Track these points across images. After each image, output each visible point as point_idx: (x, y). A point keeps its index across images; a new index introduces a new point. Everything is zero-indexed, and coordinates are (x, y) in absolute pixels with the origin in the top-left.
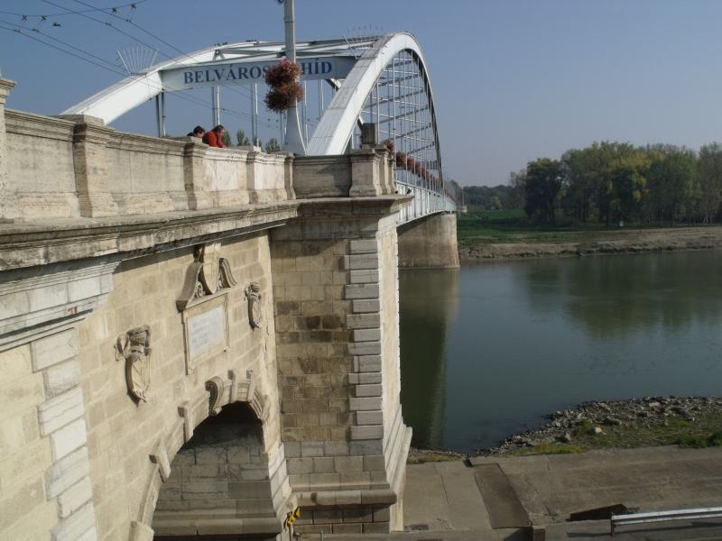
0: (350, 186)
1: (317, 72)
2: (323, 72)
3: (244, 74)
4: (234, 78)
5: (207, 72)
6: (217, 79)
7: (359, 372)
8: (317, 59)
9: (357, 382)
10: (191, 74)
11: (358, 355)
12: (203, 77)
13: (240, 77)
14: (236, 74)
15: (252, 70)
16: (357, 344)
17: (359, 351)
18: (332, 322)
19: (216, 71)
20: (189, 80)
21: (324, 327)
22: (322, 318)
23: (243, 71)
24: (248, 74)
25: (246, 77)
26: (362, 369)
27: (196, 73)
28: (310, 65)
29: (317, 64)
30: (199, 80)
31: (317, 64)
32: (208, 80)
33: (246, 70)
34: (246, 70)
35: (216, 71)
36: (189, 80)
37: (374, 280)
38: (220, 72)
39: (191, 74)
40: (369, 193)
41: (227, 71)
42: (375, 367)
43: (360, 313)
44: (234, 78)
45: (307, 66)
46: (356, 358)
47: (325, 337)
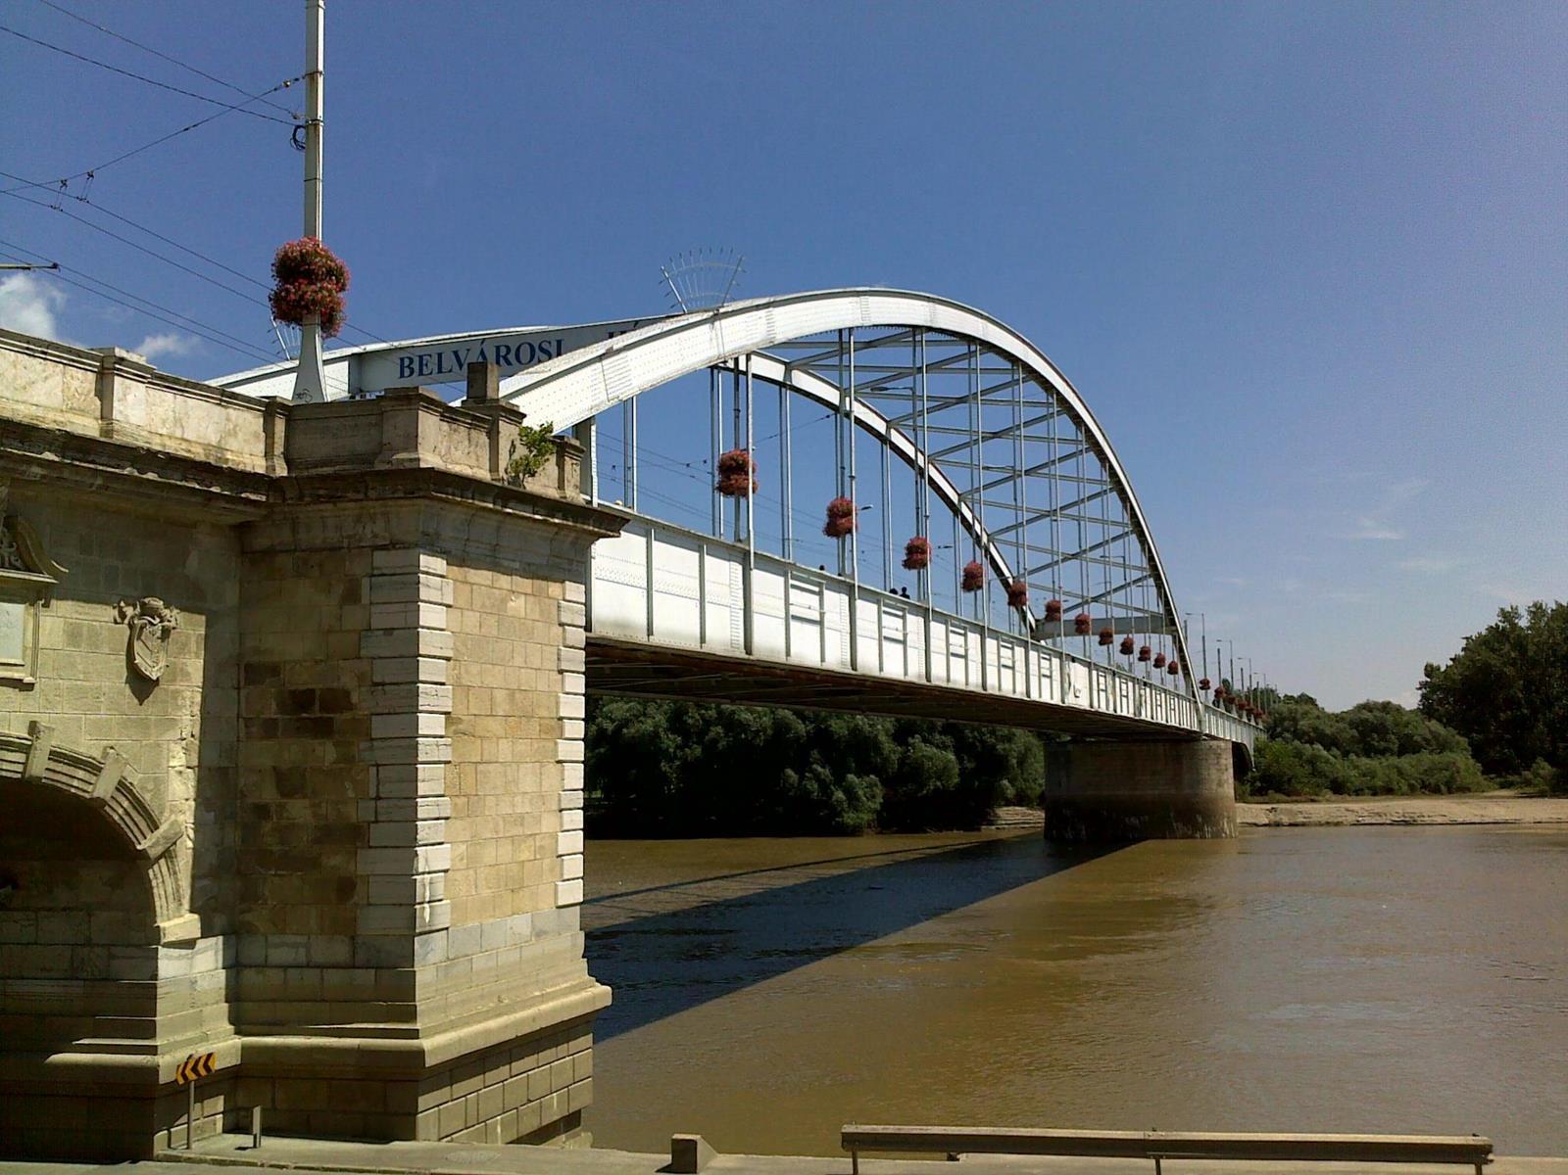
3: (505, 358)
6: (456, 368)
7: (378, 798)
9: (373, 819)
10: (411, 360)
11: (378, 765)
12: (433, 365)
15: (518, 350)
16: (375, 743)
18: (338, 700)
19: (456, 353)
20: (407, 372)
22: (318, 693)
23: (503, 351)
24: (511, 357)
25: (509, 363)
27: (421, 357)
30: (425, 371)
32: (440, 371)
35: (456, 353)
36: (407, 372)
38: (462, 356)
39: (411, 360)
43: (383, 684)
47: (323, 729)
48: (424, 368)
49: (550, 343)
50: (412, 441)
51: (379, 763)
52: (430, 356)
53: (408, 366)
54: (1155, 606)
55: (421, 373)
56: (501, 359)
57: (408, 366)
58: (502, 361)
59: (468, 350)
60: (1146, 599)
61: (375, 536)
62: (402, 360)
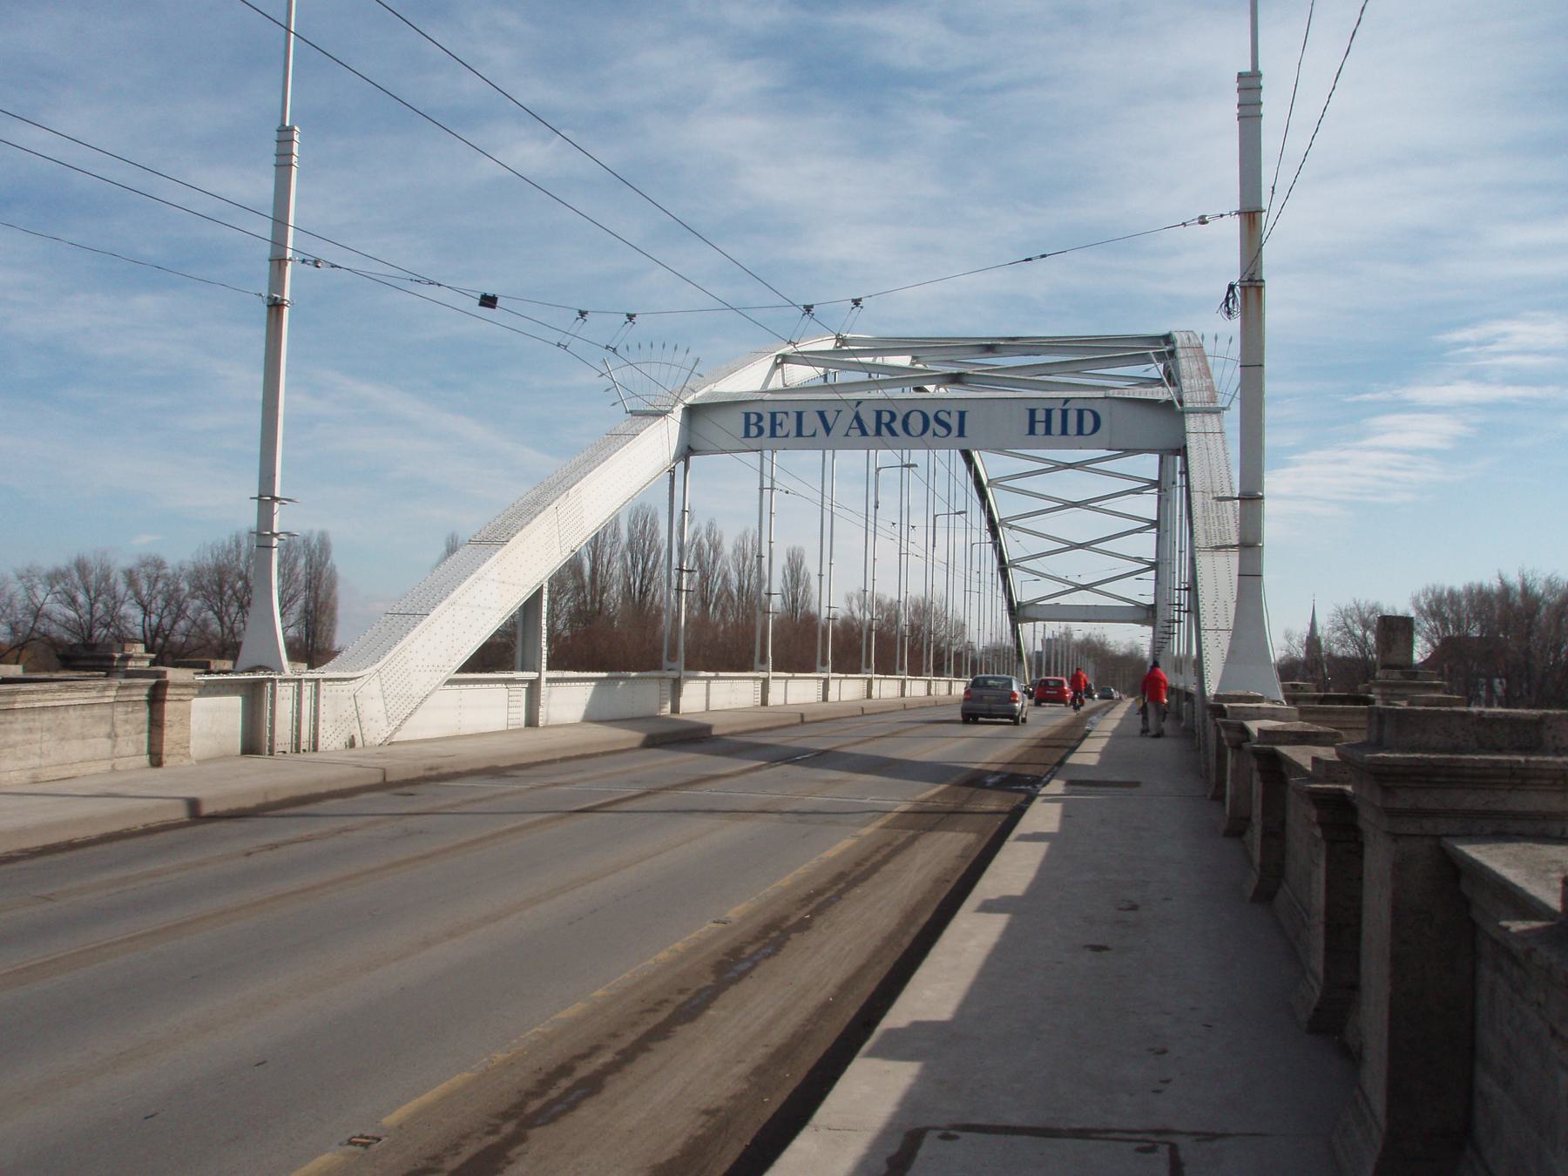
1: (1064, 432)
2: (1080, 432)
3: (888, 426)
4: (864, 433)
5: (799, 415)
6: (821, 431)
8: (1067, 400)
10: (760, 417)
12: (790, 424)
13: (878, 433)
14: (870, 424)
15: (907, 416)
19: (821, 414)
20: (754, 430)
23: (886, 418)
24: (897, 426)
25: (893, 433)
27: (773, 415)
28: (1049, 412)
29: (1065, 413)
30: (779, 431)
31: (1065, 413)
32: (799, 434)
33: (893, 417)
34: (893, 417)
35: (821, 414)
36: (754, 430)
39: (760, 417)
41: (847, 418)
44: (864, 433)
45: (1040, 416)
48: (778, 427)
49: (949, 413)
52: (786, 413)
53: (755, 424)
56: (883, 427)
57: (755, 424)
58: (884, 430)
59: (839, 412)
62: (747, 416)
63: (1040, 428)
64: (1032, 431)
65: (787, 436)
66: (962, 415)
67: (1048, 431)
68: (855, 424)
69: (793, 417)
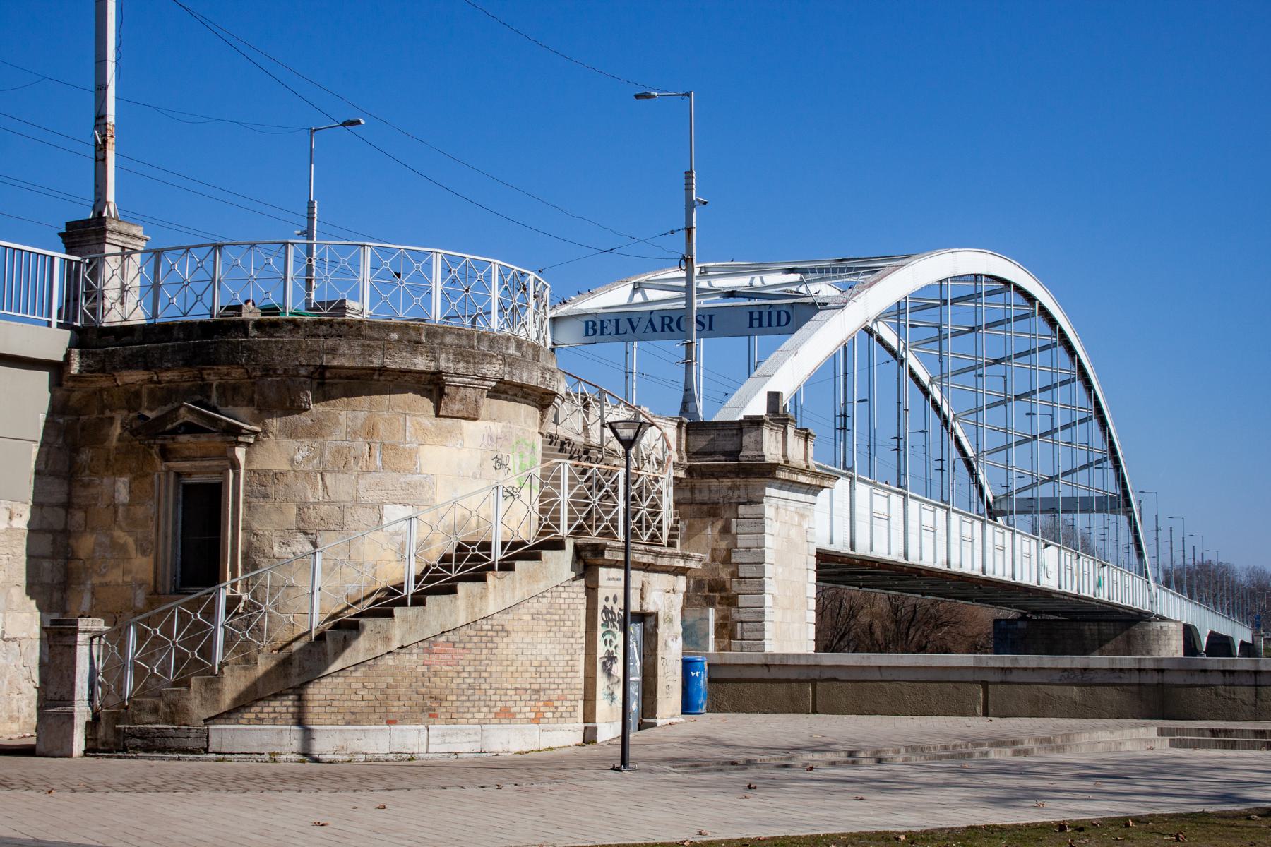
0: (740, 451)
1: (770, 325)
2: (779, 324)
4: (655, 331)
5: (617, 321)
6: (630, 330)
8: (771, 305)
10: (594, 324)
11: (742, 622)
12: (611, 328)
13: (663, 330)
14: (658, 327)
17: (743, 617)
19: (630, 320)
21: (709, 591)
23: (667, 321)
24: (674, 326)
25: (671, 330)
26: (746, 635)
27: (602, 322)
28: (761, 313)
32: (617, 333)
35: (630, 320)
36: (591, 332)
37: (762, 546)
39: (594, 324)
40: (759, 458)
41: (644, 323)
42: (757, 635)
43: (745, 578)
44: (655, 331)
45: (756, 316)
46: (739, 625)
50: (759, 443)
51: (743, 620)
54: (1112, 489)
55: (602, 333)
58: (666, 328)
60: (1102, 481)
61: (739, 497)
62: (587, 323)
63: (756, 323)
64: (751, 325)
65: (610, 334)
66: (711, 317)
67: (760, 325)
68: (649, 326)
69: (613, 323)
